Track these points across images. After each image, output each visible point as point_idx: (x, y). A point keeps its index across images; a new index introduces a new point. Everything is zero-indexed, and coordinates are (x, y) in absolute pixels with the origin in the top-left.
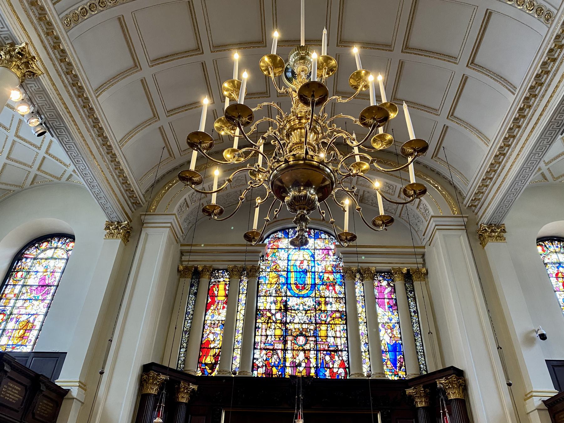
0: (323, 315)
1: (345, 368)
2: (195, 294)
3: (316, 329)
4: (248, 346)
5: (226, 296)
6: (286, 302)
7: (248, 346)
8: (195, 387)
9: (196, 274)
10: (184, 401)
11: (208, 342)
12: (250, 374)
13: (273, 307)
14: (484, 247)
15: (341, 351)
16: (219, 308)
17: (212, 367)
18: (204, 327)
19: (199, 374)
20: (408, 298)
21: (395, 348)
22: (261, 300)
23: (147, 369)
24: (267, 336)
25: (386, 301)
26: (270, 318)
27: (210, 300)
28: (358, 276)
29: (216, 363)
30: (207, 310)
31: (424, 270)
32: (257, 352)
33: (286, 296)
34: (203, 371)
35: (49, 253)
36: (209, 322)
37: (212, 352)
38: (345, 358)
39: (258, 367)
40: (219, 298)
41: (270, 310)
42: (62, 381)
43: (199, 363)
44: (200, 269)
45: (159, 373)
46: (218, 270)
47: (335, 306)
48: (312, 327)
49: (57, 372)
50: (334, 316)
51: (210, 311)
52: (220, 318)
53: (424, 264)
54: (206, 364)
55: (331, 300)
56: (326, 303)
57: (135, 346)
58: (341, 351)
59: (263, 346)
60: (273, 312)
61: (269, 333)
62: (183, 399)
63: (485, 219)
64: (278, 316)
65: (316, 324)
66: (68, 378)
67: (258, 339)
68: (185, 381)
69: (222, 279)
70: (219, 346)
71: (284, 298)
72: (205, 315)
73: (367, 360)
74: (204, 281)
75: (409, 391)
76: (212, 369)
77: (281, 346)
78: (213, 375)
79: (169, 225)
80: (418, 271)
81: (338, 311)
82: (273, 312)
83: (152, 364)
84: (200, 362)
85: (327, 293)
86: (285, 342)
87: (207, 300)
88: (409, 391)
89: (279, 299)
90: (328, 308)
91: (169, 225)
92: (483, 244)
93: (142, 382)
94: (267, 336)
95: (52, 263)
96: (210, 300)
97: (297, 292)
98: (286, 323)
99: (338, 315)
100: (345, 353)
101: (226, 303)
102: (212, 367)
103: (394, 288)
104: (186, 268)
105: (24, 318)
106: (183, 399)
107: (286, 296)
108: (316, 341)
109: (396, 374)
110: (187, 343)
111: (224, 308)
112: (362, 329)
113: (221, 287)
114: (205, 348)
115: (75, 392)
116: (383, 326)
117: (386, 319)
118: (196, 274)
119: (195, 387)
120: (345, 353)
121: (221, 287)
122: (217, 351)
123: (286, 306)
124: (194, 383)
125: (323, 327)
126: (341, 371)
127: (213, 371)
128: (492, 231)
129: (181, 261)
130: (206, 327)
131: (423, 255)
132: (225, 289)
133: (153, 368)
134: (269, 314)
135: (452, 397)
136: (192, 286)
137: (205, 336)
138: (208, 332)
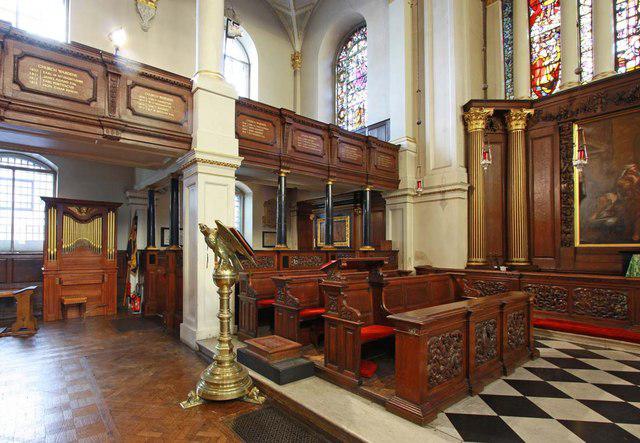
8: (531, 111)
11: (541, 60)
16: (548, 15)
17: (551, 85)
18: (531, 47)
19: (535, 97)
23: (466, 108)
27: (532, 12)
34: (538, 93)
35: (355, 49)
36: (536, 39)
39: (626, 61)
42: (393, 140)
43: (532, 87)
49: (387, 133)
51: (535, 25)
54: (541, 85)
62: (517, 126)
66: (398, 134)
68: (515, 108)
70: (557, 59)
72: (530, 32)
83: (471, 102)
84: (533, 85)
87: (529, 13)
93: (465, 122)
95: (359, 56)
96: (532, 12)
105: (356, 107)
106: (517, 126)
111: (555, 12)
115: (404, 144)
119: (531, 111)
122: (555, 66)
130: (534, 45)
133: (474, 104)
137: (534, 55)
138: (537, 50)
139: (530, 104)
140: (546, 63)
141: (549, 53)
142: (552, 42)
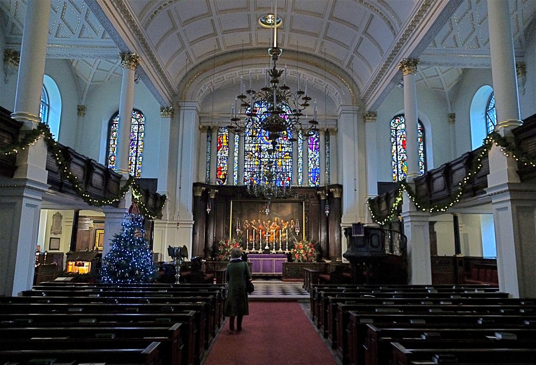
0: (280, 154)
1: (290, 181)
2: (210, 142)
3: (276, 161)
4: (241, 170)
5: (227, 143)
6: (260, 146)
7: (241, 170)
9: (210, 130)
10: (213, 197)
11: (221, 168)
12: (242, 184)
13: (253, 149)
14: (365, 123)
15: (288, 172)
17: (224, 180)
20: (325, 144)
21: (314, 171)
22: (247, 145)
23: (195, 185)
24: (250, 165)
25: (314, 146)
26: (252, 155)
28: (300, 132)
29: (225, 178)
30: (218, 151)
31: (336, 129)
32: (246, 173)
33: (260, 143)
34: (219, 182)
37: (223, 173)
38: (290, 176)
40: (224, 144)
41: (252, 151)
44: (212, 128)
45: (201, 186)
46: (222, 128)
47: (287, 149)
48: (274, 160)
50: (286, 154)
52: (225, 155)
53: (337, 125)
54: (220, 179)
55: (284, 146)
56: (282, 148)
57: (188, 176)
58: (288, 172)
59: (249, 170)
60: (254, 152)
61: (251, 163)
63: (368, 109)
64: (256, 154)
65: (276, 158)
67: (246, 166)
68: (213, 189)
69: (224, 133)
71: (259, 145)
73: (301, 177)
74: (214, 134)
75: (318, 192)
76: (224, 181)
77: (258, 170)
78: (224, 184)
79: (195, 108)
80: (332, 130)
81: (288, 152)
82: (254, 152)
84: (217, 178)
85: (283, 142)
86: (260, 168)
88: (318, 192)
89: (257, 145)
90: (283, 150)
91: (195, 108)
92: (365, 121)
94: (250, 165)
97: (266, 141)
98: (260, 158)
99: (288, 154)
100: (290, 173)
101: (228, 147)
102: (224, 180)
103: (319, 138)
104: (204, 127)
107: (260, 143)
108: (276, 168)
109: (315, 184)
110: (210, 168)
112: (300, 161)
113: (224, 137)
114: (219, 170)
116: (311, 160)
117: (313, 156)
118: (210, 130)
120: (290, 173)
121: (224, 137)
123: (260, 149)
124: (217, 189)
125: (280, 160)
126: (288, 182)
127: (224, 182)
128: (370, 116)
129: (200, 123)
131: (337, 120)
132: (226, 139)
134: (251, 153)
135: (335, 197)
136: (208, 137)
139: (216, 187)
140: (222, 170)
141: (224, 166)
142: (225, 162)
